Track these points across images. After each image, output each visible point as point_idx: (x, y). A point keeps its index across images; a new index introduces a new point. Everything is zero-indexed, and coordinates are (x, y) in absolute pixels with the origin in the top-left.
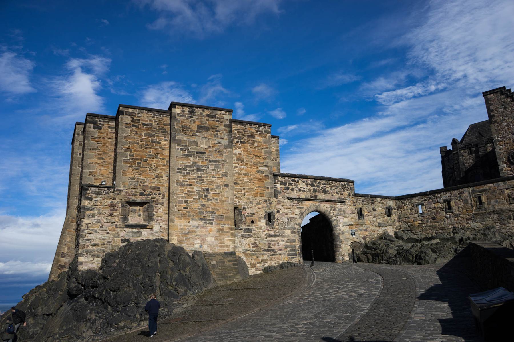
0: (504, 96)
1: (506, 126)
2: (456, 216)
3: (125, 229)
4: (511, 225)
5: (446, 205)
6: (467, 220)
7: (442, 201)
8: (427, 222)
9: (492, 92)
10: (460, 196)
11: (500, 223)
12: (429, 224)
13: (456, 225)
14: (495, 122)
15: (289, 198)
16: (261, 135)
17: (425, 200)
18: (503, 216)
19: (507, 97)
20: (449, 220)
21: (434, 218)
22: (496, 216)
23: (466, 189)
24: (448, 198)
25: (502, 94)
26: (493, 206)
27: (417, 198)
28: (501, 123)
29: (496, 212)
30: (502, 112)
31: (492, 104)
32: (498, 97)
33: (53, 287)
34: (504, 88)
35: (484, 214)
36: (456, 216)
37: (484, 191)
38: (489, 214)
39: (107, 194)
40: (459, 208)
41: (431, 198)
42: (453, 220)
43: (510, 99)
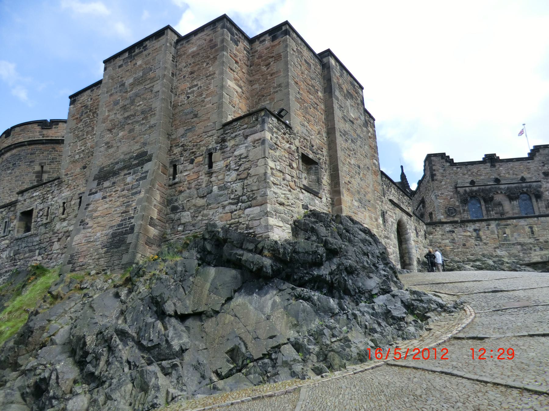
0: (444, 160)
1: (445, 185)
2: (486, 244)
3: (303, 191)
4: (532, 255)
5: (474, 234)
6: (495, 248)
7: (471, 230)
8: (458, 248)
9: (435, 155)
10: (488, 228)
11: (524, 253)
12: (460, 250)
13: (485, 252)
14: (436, 180)
15: (391, 201)
16: (371, 127)
17: (456, 228)
18: (525, 247)
19: (447, 161)
20: (478, 247)
21: (464, 245)
22: (519, 247)
23: (493, 222)
24: (477, 228)
25: (443, 158)
26: (516, 238)
27: (448, 225)
28: (441, 182)
29: (519, 244)
30: (443, 173)
31: (434, 165)
32: (439, 160)
33: (179, 269)
34: (444, 154)
35: (509, 244)
36: (486, 244)
37: (508, 225)
38: (514, 244)
39: (284, 134)
40: (487, 237)
41: (461, 227)
42: (482, 247)
43: (448, 164)
